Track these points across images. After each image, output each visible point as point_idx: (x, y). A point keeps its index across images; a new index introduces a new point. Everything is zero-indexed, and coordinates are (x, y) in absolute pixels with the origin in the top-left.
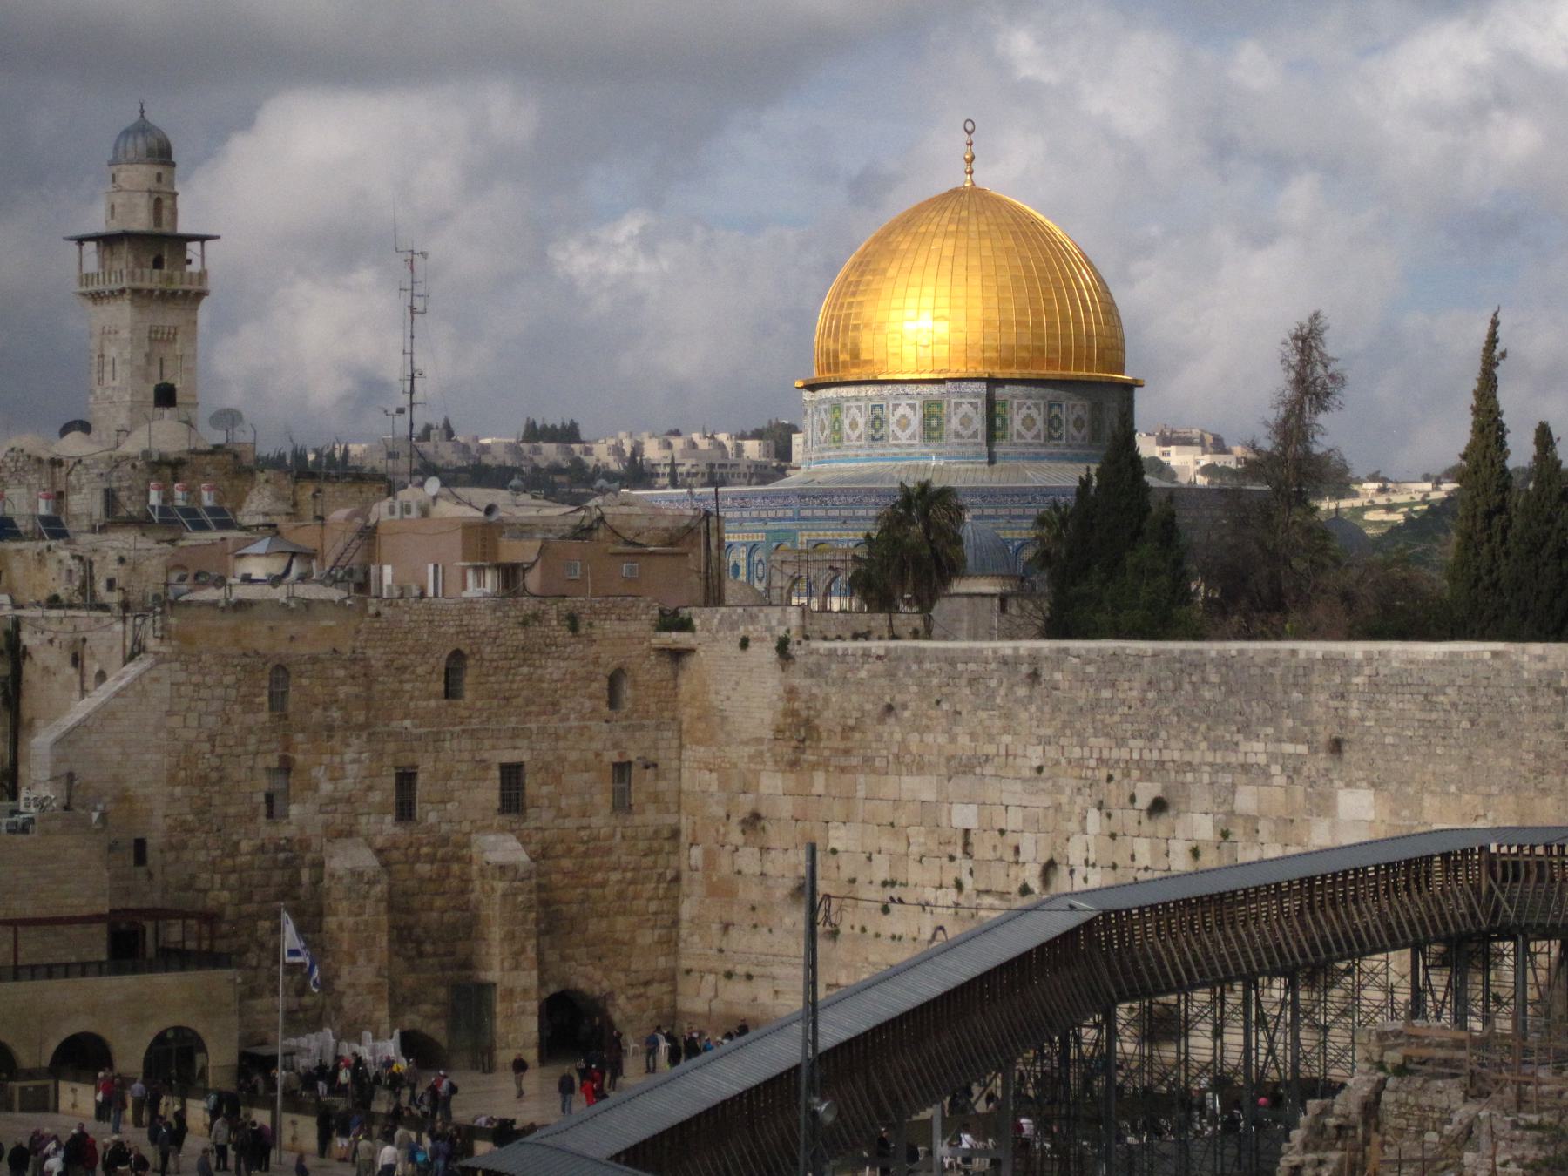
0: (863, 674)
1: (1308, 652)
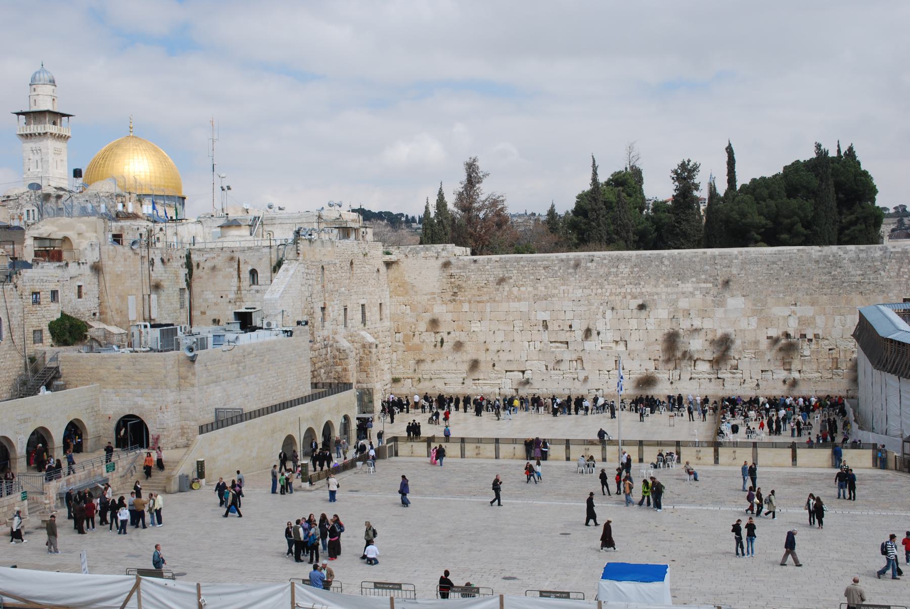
0: (488, 267)
1: (711, 253)
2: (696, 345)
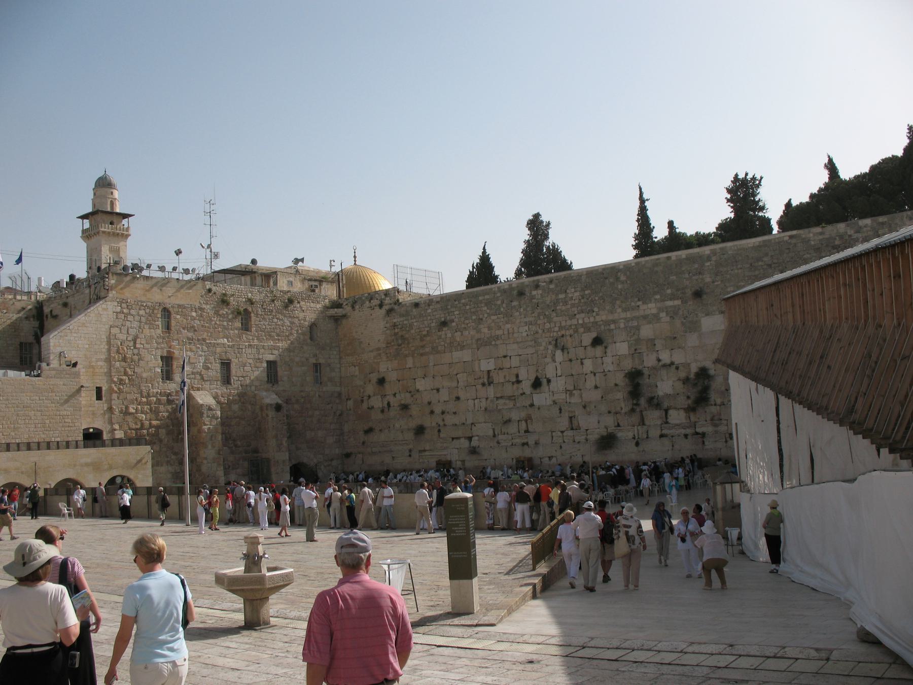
1: (676, 256)
2: (666, 386)
